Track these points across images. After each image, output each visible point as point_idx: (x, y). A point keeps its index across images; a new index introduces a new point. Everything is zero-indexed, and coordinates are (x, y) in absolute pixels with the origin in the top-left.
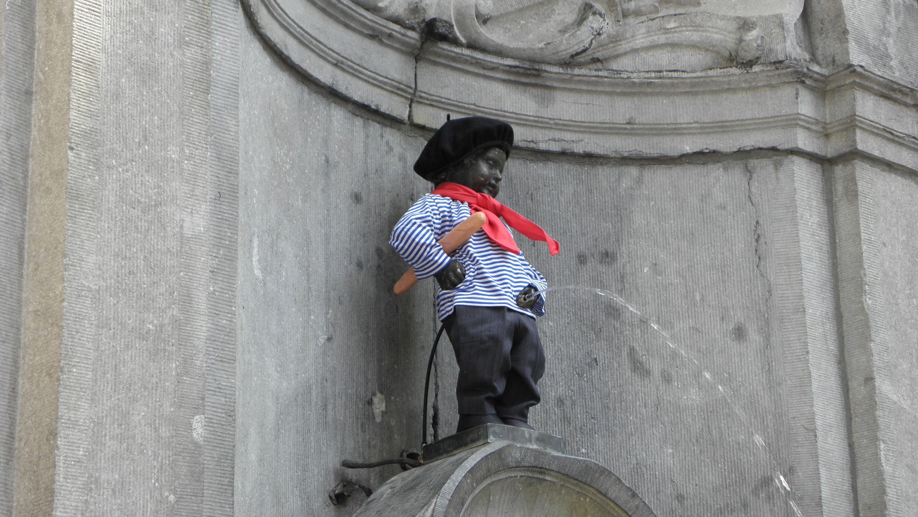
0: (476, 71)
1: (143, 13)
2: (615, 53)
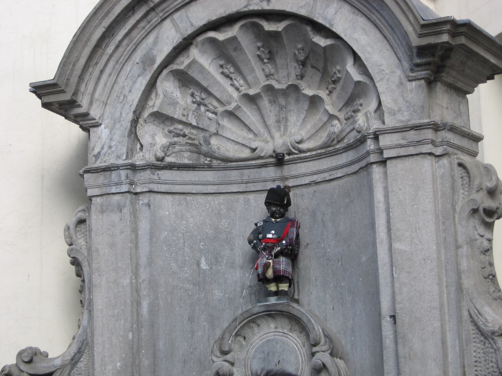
0: (302, 161)
1: (110, 229)
2: (343, 136)
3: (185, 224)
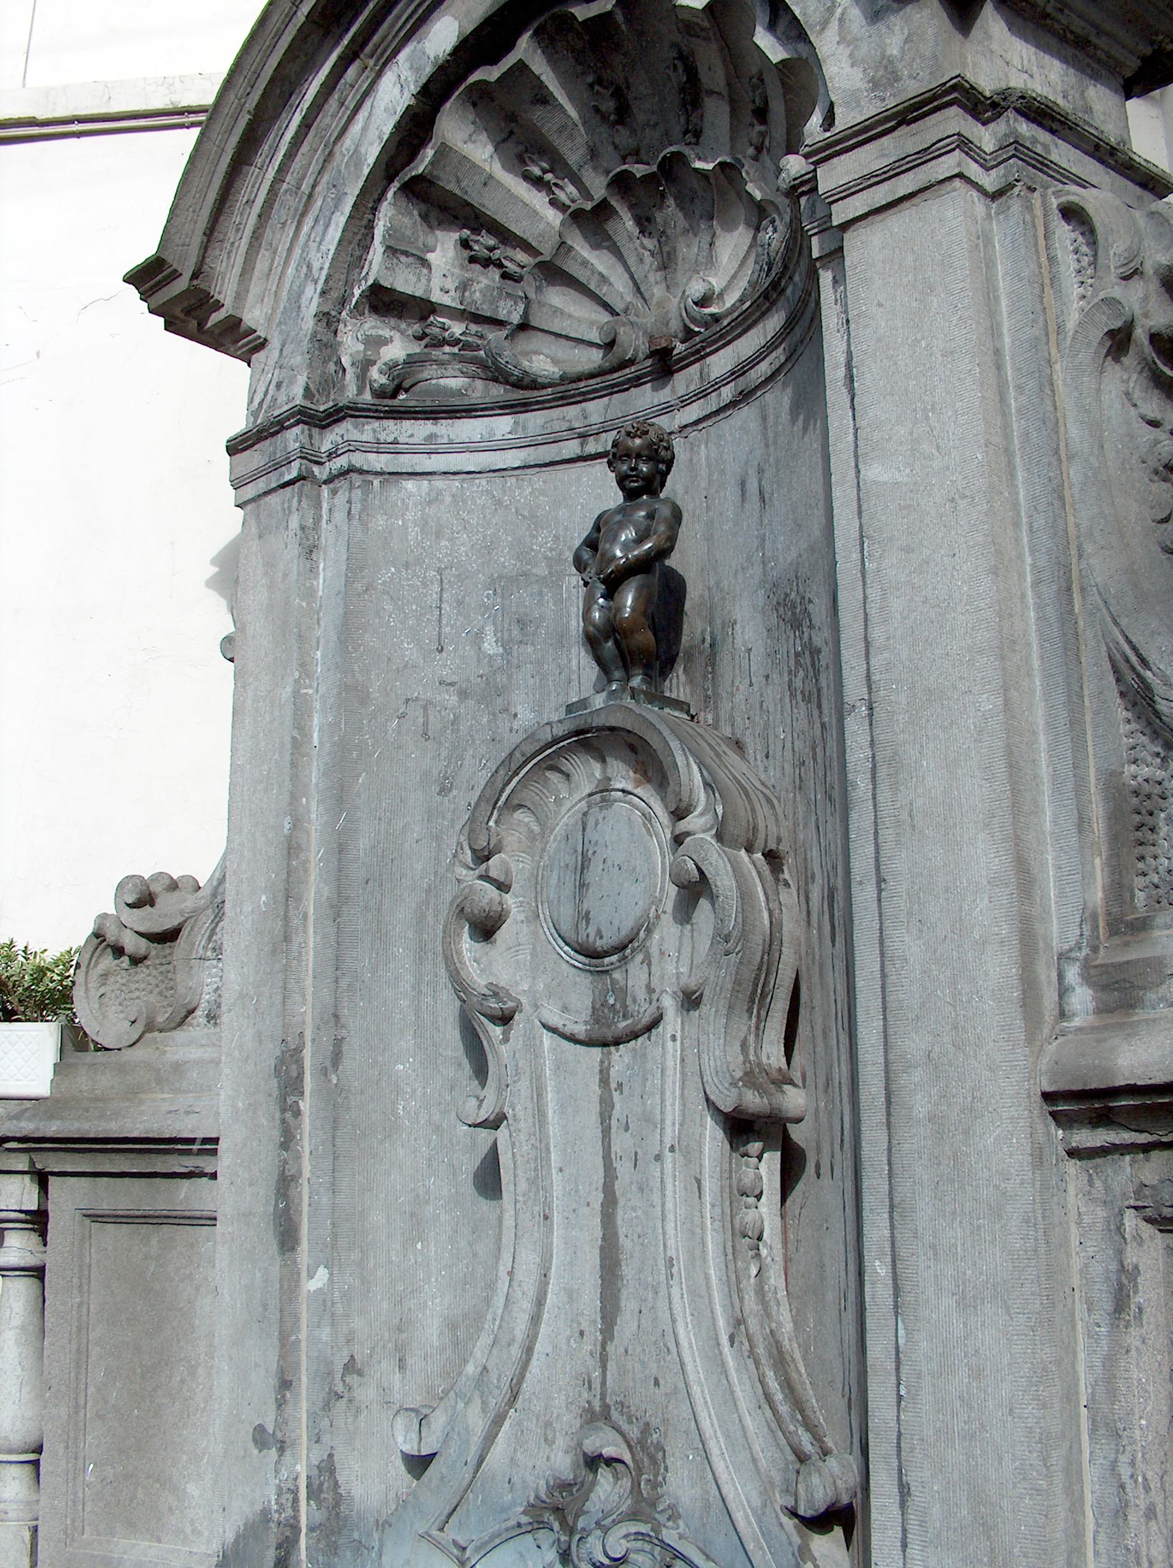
3: (447, 548)
